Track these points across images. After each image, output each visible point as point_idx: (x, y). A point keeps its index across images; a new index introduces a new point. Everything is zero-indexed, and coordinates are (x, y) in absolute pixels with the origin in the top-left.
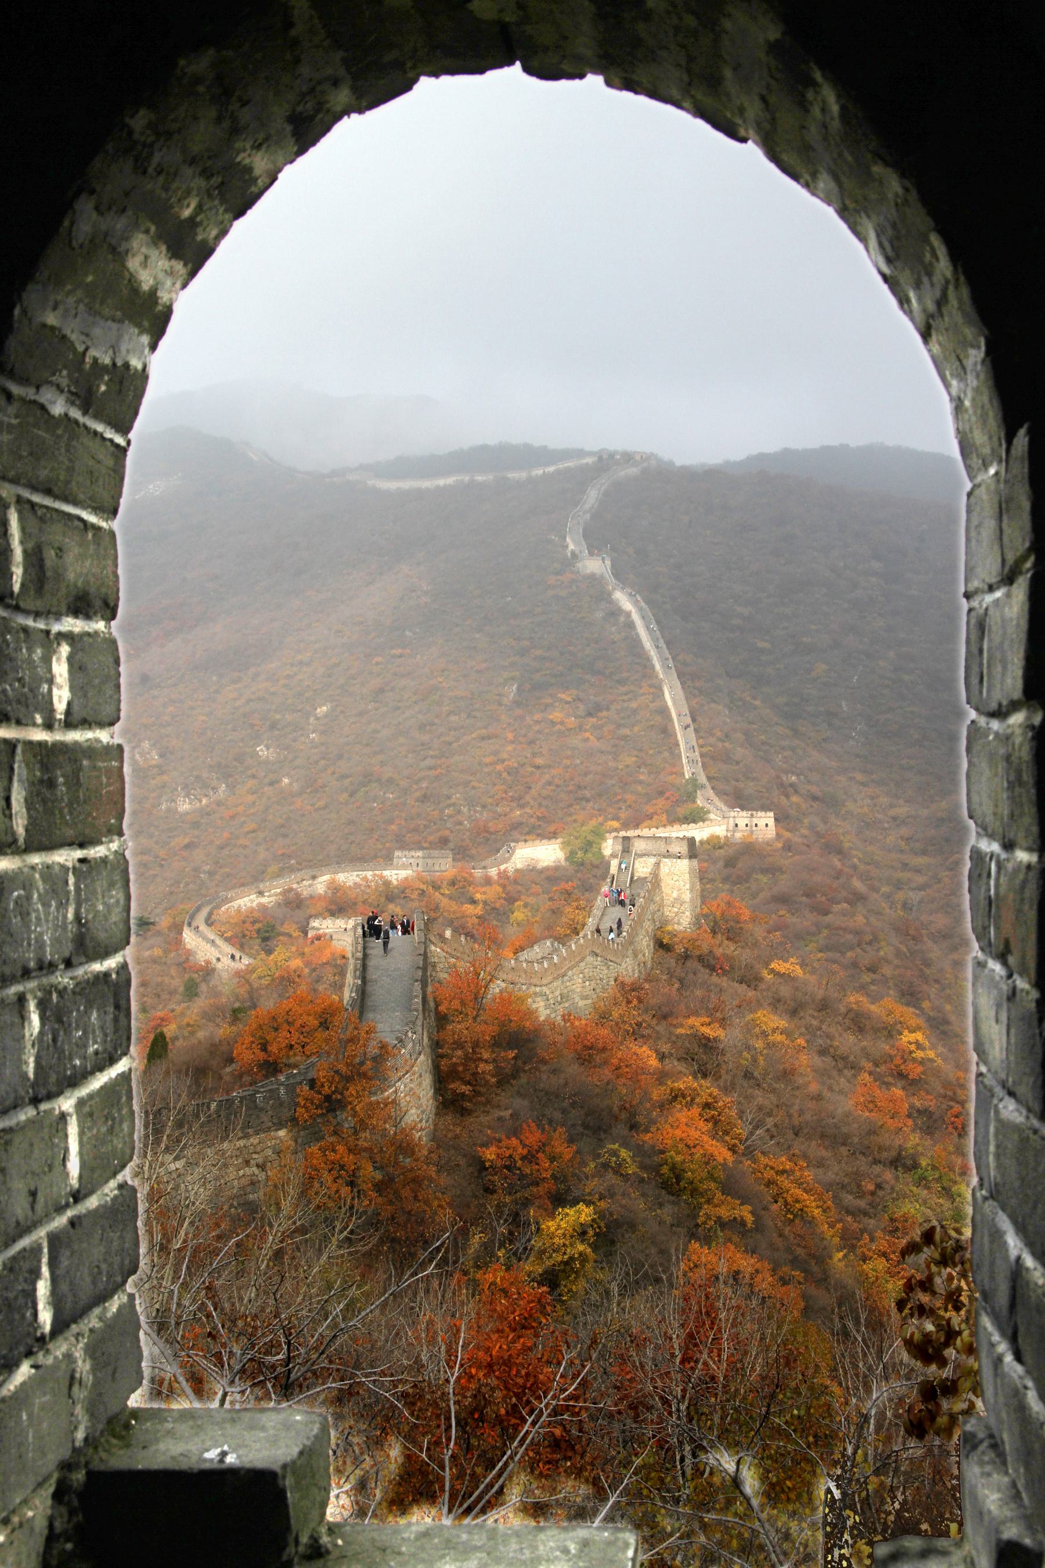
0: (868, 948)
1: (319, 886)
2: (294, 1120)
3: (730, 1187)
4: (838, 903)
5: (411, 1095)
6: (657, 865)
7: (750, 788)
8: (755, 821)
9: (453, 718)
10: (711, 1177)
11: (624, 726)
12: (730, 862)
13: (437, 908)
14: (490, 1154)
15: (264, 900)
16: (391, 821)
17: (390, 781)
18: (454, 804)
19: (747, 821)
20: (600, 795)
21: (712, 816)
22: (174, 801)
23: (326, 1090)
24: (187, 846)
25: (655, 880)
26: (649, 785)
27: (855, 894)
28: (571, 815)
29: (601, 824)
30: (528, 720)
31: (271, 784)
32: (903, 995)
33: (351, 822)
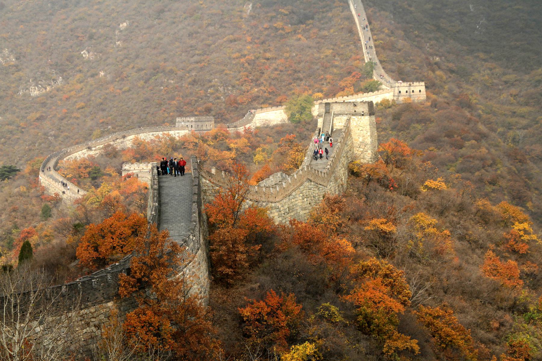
0: (490, 169)
1: (128, 143)
2: (118, 295)
3: (403, 328)
4: (469, 140)
5: (194, 276)
6: (349, 120)
7: (408, 67)
8: (412, 88)
9: (211, 28)
10: (391, 322)
11: (324, 29)
12: (396, 117)
13: (206, 154)
14: (246, 312)
15: (92, 153)
16: (173, 98)
17: (171, 71)
18: (214, 86)
19: (407, 89)
20: (310, 76)
21: (383, 87)
22: (27, 89)
23: (138, 275)
24: (38, 119)
25: (347, 131)
26: (342, 68)
27: (479, 134)
28: (291, 90)
29: (311, 95)
30: (260, 28)
31: (93, 76)
32: (514, 199)
33: (147, 100)
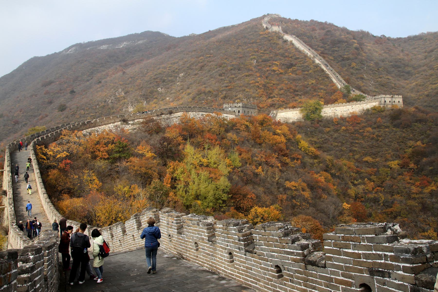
17: (209, 92)
